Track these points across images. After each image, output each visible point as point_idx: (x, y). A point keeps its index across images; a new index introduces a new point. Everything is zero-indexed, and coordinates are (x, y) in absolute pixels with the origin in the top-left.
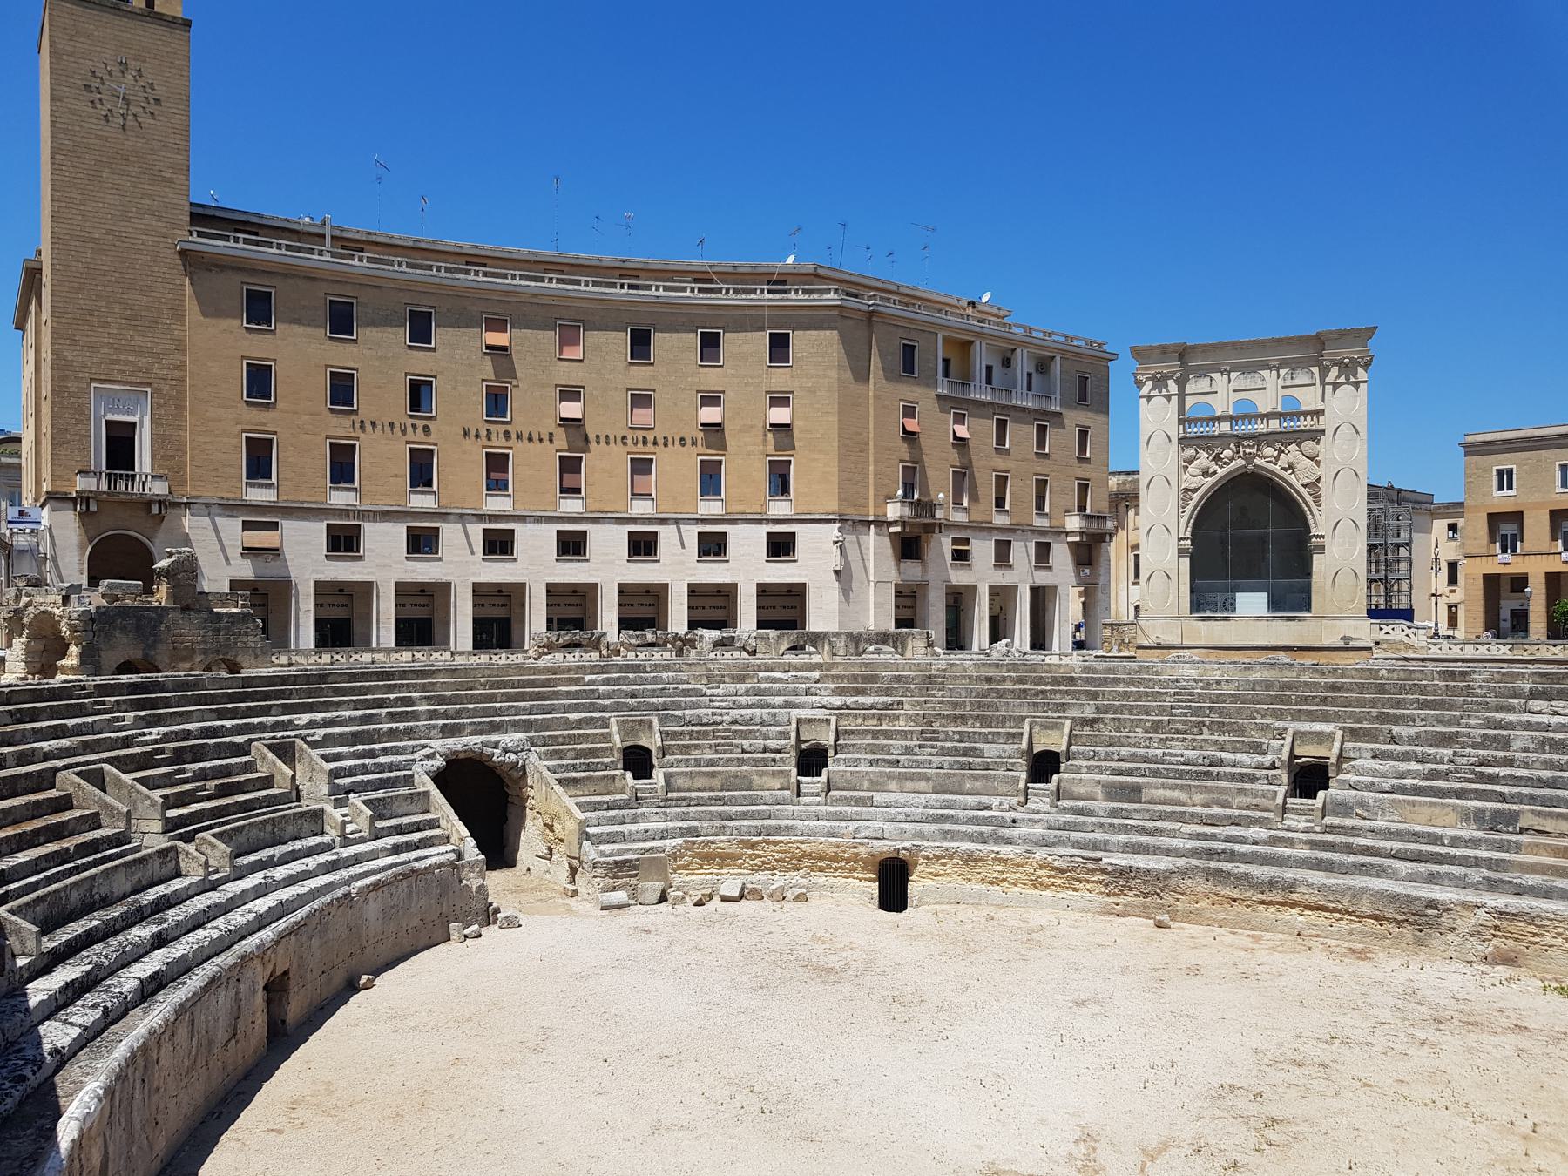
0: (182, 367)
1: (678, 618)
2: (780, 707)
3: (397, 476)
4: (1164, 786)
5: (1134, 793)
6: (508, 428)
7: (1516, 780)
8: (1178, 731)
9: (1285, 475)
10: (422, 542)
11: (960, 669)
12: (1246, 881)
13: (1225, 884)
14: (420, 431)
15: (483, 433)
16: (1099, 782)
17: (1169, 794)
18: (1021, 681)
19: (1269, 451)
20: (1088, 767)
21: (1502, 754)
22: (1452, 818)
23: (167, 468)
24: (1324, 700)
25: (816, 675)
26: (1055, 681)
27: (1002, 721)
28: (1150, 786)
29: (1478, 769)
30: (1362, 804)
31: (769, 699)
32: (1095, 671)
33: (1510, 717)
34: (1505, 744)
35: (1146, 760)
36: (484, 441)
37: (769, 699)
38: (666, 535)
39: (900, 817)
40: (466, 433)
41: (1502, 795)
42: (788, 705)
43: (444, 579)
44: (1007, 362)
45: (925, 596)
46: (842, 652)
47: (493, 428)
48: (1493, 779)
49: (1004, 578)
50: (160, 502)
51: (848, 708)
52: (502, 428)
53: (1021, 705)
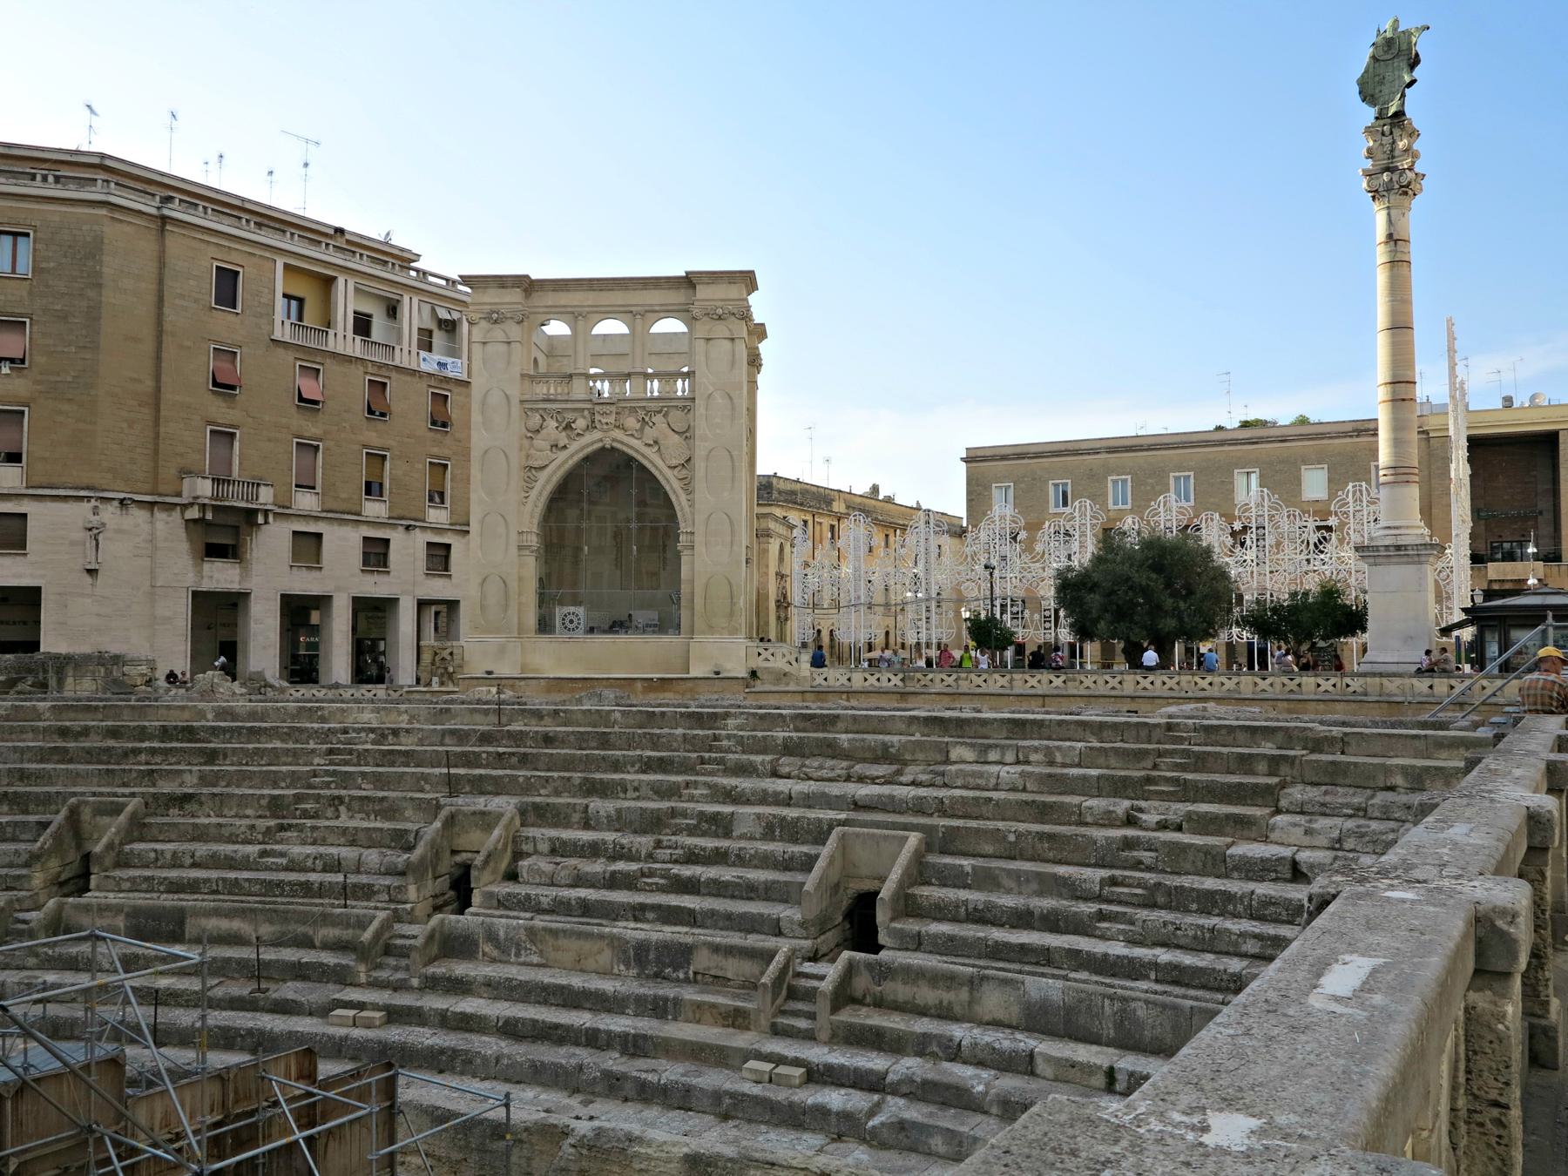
4: (217, 913)
5: (170, 927)
7: (719, 889)
8: (305, 814)
16: (117, 910)
17: (224, 925)
18: (114, 733)
19: (631, 422)
20: (132, 880)
21: (709, 843)
22: (606, 957)
24: (524, 760)
26: (165, 733)
27: (46, 801)
28: (199, 913)
29: (676, 869)
30: (491, 937)
33: (745, 784)
41: (691, 912)
44: (392, 310)
45: (247, 608)
49: (375, 587)
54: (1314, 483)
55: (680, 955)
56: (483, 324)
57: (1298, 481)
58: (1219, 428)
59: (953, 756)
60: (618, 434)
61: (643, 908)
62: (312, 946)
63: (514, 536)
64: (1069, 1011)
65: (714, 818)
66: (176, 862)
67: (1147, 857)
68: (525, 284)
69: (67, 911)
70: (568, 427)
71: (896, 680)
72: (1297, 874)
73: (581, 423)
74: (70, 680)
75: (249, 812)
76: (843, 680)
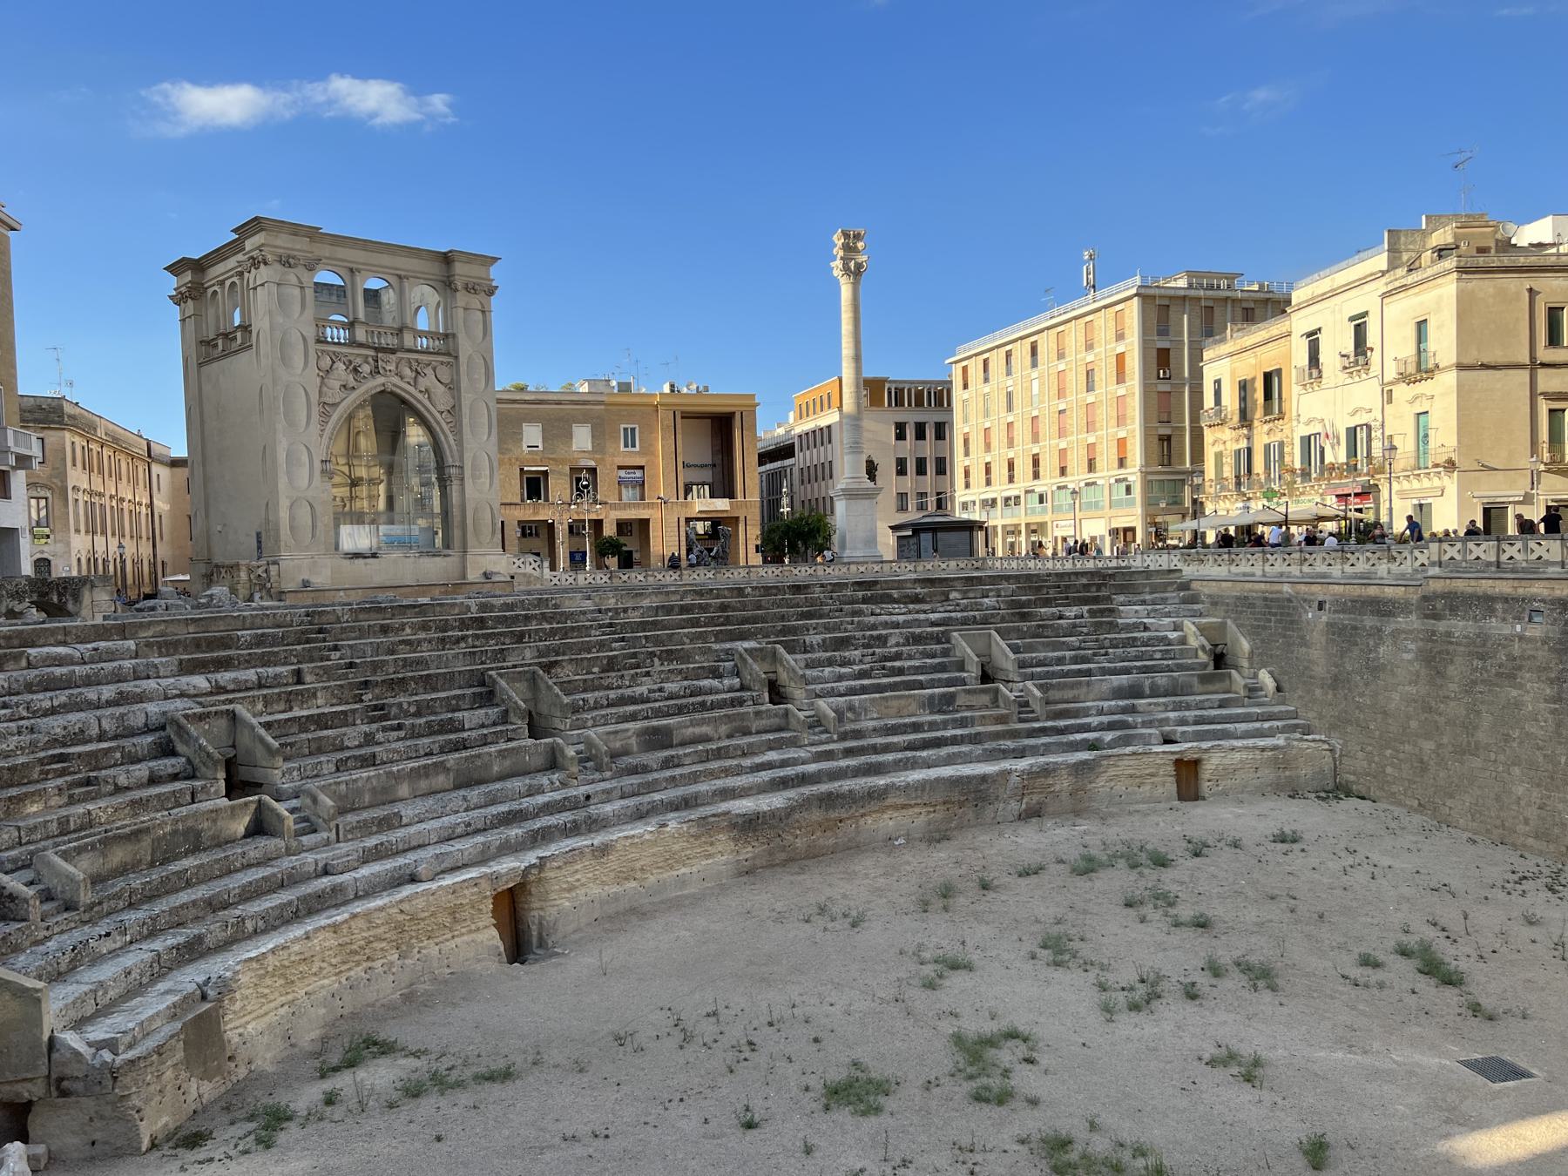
2: (109, 704)
9: (424, 398)
11: (332, 618)
12: (851, 798)
13: (834, 808)
17: (698, 730)
22: (913, 707)
25: (131, 644)
28: (681, 726)
30: (851, 708)
31: (91, 694)
32: (491, 608)
34: (882, 641)
35: (633, 700)
37: (91, 694)
39: (459, 830)
41: (920, 682)
42: (122, 699)
48: (901, 672)
51: (219, 689)
53: (456, 656)
54: (582, 438)
55: (949, 699)
56: (278, 266)
57: (570, 436)
58: (522, 389)
59: (951, 596)
60: (396, 380)
61: (896, 684)
62: (750, 733)
63: (317, 465)
64: (1131, 687)
65: (879, 637)
66: (597, 706)
67: (1085, 630)
68: (313, 234)
70: (355, 370)
71: (605, 579)
72: (1146, 629)
73: (366, 369)
75: (596, 670)
76: (571, 580)
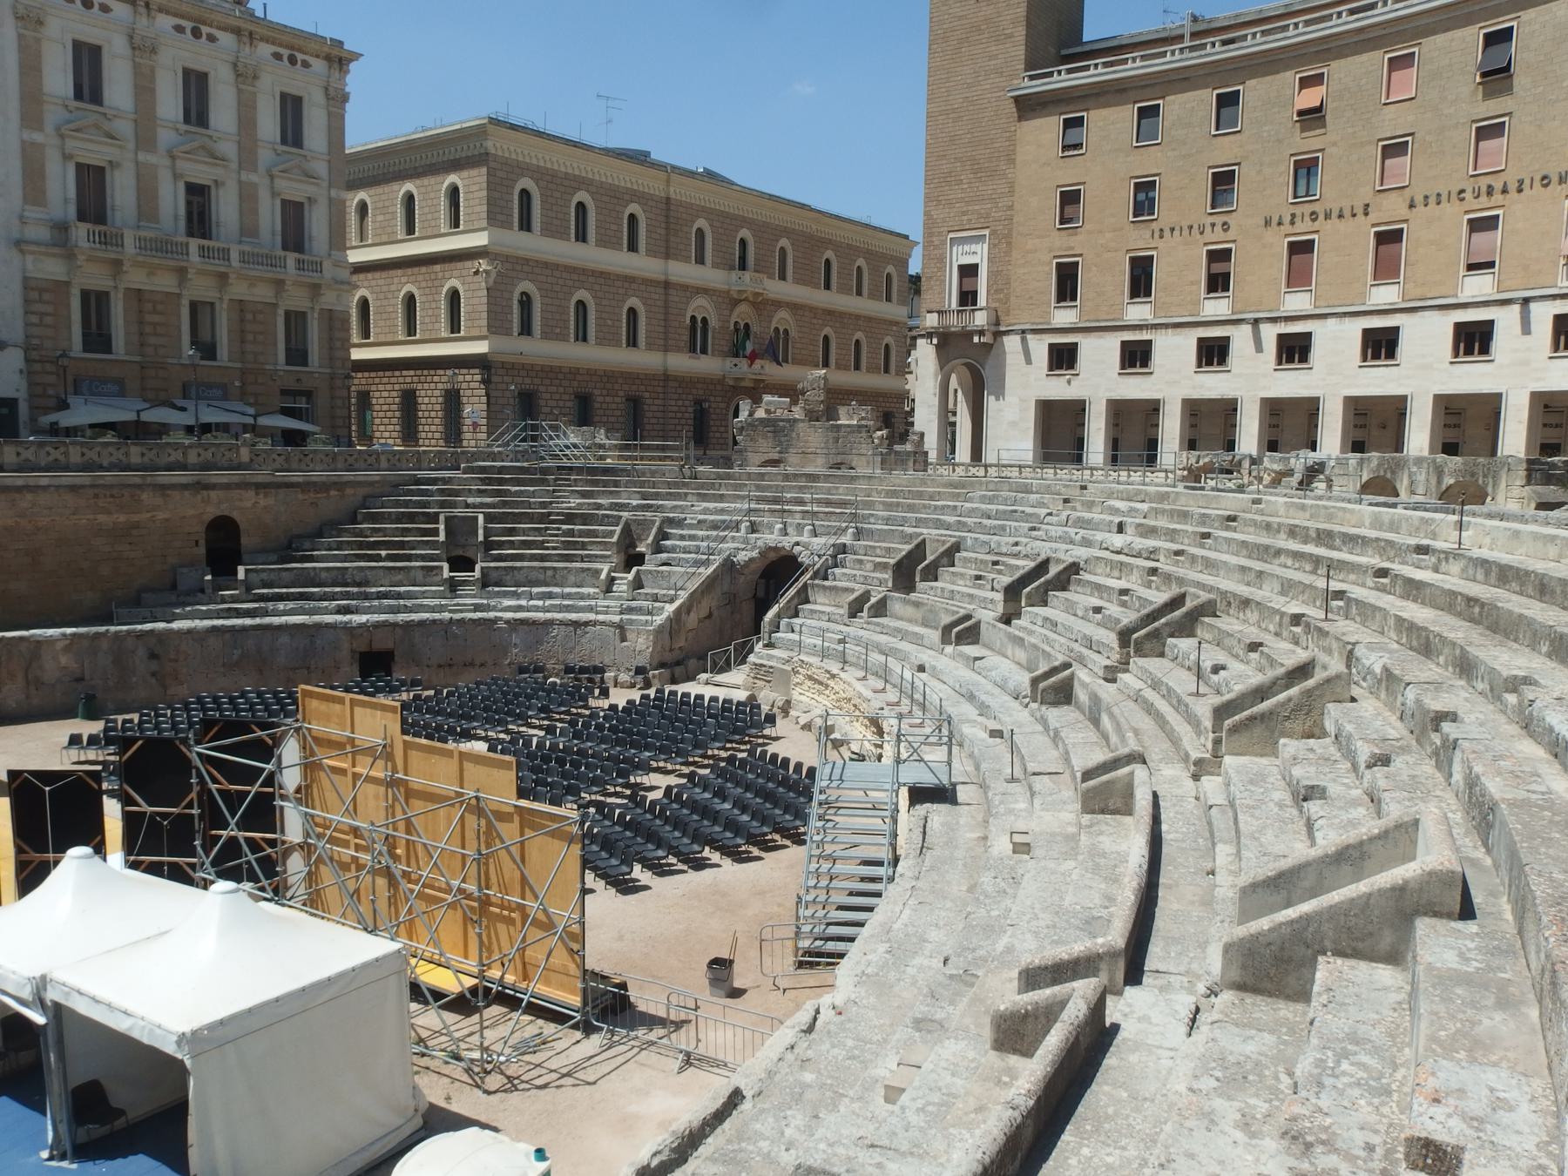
0: (1011, 208)
1: (1248, 438)
3: (1192, 283)
6: (1316, 207)
10: (1213, 353)
14: (1218, 228)
15: (1287, 219)
23: (999, 300)
36: (1287, 228)
37: (1072, 531)
38: (1506, 321)
40: (1268, 223)
43: (1230, 394)
46: (1421, 490)
47: (1298, 210)
50: (981, 333)
52: (1308, 209)
69: (1076, 683)
74: (1503, 485)
